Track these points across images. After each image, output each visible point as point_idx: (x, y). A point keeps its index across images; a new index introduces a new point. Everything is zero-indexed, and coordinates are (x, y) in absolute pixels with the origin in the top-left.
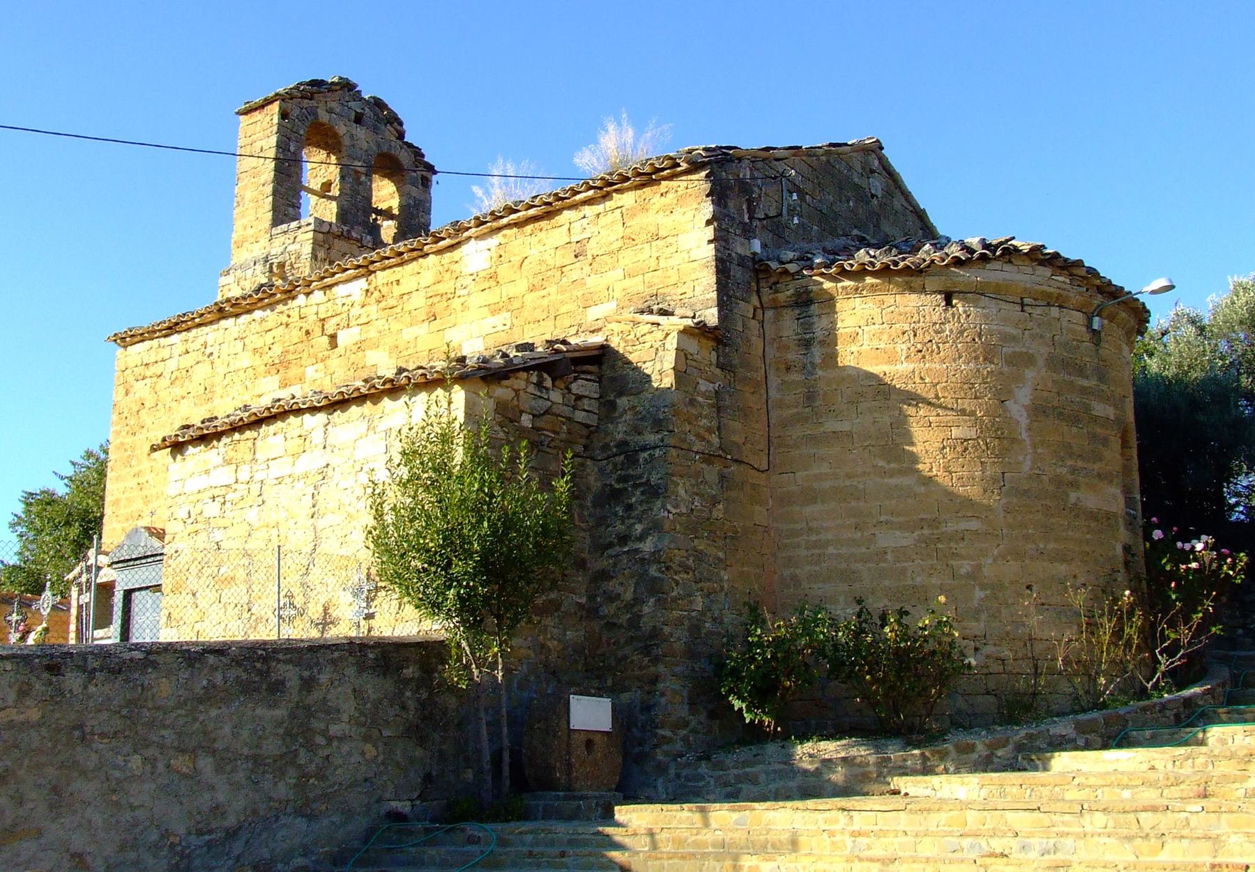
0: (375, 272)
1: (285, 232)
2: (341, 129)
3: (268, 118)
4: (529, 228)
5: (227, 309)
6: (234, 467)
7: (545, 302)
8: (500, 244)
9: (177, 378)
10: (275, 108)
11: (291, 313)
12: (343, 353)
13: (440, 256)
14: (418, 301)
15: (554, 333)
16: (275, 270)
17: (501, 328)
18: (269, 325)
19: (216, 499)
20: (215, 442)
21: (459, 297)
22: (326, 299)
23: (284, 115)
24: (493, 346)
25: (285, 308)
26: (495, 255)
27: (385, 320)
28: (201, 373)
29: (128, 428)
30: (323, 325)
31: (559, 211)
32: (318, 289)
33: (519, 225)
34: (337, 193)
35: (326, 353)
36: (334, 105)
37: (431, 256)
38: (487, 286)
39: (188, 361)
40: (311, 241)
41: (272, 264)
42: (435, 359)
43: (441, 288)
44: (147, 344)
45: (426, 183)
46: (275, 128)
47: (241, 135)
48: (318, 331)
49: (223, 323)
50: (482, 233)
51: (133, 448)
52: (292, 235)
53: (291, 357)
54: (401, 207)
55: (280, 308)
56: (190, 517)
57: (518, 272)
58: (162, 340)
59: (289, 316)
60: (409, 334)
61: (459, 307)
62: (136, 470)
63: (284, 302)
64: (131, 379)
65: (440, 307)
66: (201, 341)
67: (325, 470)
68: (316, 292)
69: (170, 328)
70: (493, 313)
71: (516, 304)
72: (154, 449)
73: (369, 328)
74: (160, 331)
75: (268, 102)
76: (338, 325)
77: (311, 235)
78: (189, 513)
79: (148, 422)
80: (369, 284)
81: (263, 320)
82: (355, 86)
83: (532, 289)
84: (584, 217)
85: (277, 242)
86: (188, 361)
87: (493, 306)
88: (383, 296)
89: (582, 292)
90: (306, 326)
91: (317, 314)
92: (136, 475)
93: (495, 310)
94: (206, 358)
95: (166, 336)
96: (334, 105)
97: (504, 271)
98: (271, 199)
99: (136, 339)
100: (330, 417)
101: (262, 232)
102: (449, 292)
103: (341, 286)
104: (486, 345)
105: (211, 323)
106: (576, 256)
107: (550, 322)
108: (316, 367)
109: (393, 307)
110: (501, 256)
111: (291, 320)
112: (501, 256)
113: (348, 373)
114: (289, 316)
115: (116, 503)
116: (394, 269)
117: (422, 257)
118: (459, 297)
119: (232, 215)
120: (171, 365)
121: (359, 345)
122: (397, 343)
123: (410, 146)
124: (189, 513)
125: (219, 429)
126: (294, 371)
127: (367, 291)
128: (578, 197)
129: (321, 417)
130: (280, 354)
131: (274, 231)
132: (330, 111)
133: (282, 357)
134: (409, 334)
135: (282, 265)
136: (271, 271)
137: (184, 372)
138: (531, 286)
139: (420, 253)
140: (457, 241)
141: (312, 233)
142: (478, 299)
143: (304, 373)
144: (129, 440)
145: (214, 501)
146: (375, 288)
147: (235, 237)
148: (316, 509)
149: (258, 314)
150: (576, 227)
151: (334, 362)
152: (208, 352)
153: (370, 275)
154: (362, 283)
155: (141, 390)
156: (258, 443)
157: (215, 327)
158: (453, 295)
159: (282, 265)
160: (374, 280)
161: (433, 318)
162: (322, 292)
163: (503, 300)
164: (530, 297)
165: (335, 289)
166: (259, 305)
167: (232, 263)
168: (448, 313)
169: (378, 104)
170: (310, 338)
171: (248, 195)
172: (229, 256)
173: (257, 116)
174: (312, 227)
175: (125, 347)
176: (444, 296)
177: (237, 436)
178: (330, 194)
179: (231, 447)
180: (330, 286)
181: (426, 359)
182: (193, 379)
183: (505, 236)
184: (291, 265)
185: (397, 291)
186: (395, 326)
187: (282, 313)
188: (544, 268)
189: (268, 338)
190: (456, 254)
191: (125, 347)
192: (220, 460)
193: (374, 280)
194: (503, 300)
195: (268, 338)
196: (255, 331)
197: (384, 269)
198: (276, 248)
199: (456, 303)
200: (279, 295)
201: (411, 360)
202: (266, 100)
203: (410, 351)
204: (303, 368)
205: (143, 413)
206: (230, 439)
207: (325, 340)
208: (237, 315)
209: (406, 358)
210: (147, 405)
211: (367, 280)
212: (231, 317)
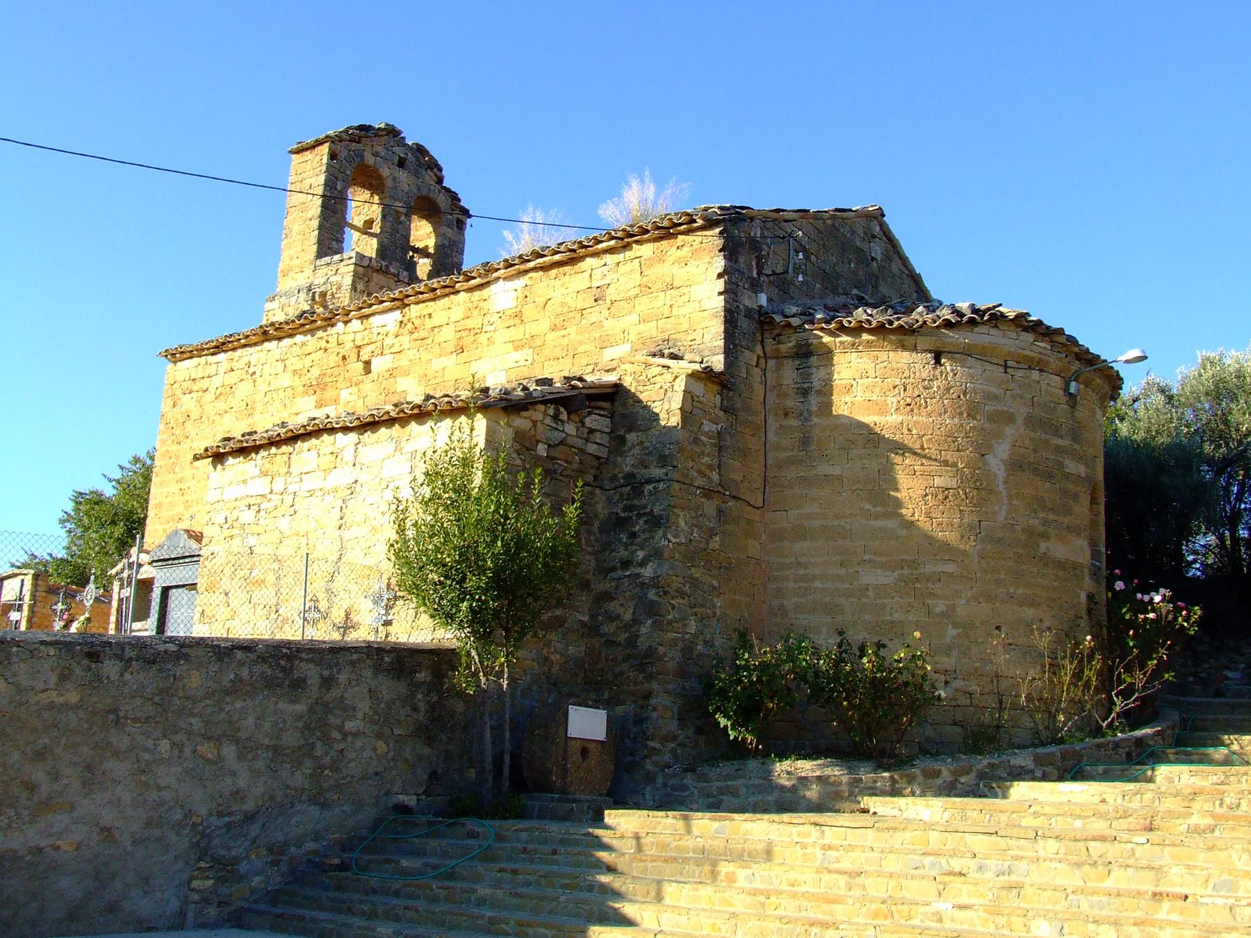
0: (409, 305)
1: (328, 264)
2: (385, 172)
3: (318, 158)
4: (553, 272)
7: (565, 341)
9: (221, 394)
10: (325, 148)
11: (330, 339)
12: (375, 378)
14: (448, 334)
16: (317, 298)
17: (522, 363)
18: (309, 348)
22: (362, 328)
23: (333, 156)
25: (325, 334)
26: (521, 296)
28: (244, 390)
29: (174, 437)
31: (582, 258)
33: (545, 268)
34: (378, 231)
35: (360, 378)
36: (380, 149)
39: (232, 378)
41: (315, 293)
43: (470, 323)
44: (196, 360)
45: (461, 226)
46: (324, 168)
47: (292, 172)
48: (353, 357)
49: (267, 345)
51: (178, 457)
52: (334, 268)
53: (327, 379)
54: (437, 246)
55: (320, 333)
57: (542, 312)
58: (210, 358)
59: (328, 342)
60: (438, 364)
62: (179, 476)
63: (324, 328)
64: (179, 392)
65: (467, 341)
66: (245, 360)
68: (354, 321)
69: (217, 347)
70: (516, 349)
71: (538, 342)
72: (197, 458)
74: (208, 349)
75: (319, 143)
79: (193, 434)
81: (303, 344)
82: (399, 133)
83: (554, 328)
85: (320, 273)
86: (232, 378)
90: (343, 352)
91: (354, 341)
92: (180, 481)
94: (249, 376)
95: (213, 354)
96: (380, 149)
97: (528, 311)
98: (316, 232)
99: (185, 356)
101: (307, 263)
103: (377, 317)
105: (256, 344)
106: (596, 301)
107: (569, 360)
108: (350, 390)
111: (329, 345)
114: (328, 342)
115: (160, 505)
117: (453, 293)
119: (280, 245)
120: (217, 381)
122: (427, 372)
123: (448, 190)
125: (258, 443)
126: (329, 393)
127: (401, 322)
128: (600, 246)
129: (353, 436)
131: (318, 262)
132: (376, 155)
134: (438, 364)
135: (323, 295)
136: (313, 299)
137: (228, 389)
140: (486, 280)
142: (503, 336)
143: (339, 395)
144: (174, 448)
146: (409, 320)
147: (281, 266)
148: (343, 521)
149: (299, 338)
150: (597, 274)
151: (368, 387)
152: (251, 371)
154: (397, 315)
155: (187, 403)
156: (293, 457)
157: (259, 348)
159: (323, 295)
164: (551, 336)
165: (372, 319)
166: (301, 330)
167: (278, 290)
168: (475, 346)
169: (420, 150)
171: (296, 228)
172: (275, 283)
173: (308, 155)
174: (353, 261)
175: (175, 362)
177: (274, 450)
178: (372, 231)
180: (367, 316)
182: (237, 395)
183: (531, 278)
184: (332, 294)
185: (429, 323)
186: (425, 356)
187: (321, 338)
188: (565, 310)
189: (308, 361)
190: (485, 293)
191: (175, 362)
192: (257, 471)
195: (308, 361)
197: (417, 303)
198: (319, 279)
199: (483, 338)
202: (317, 141)
205: (188, 424)
206: (267, 453)
207: (360, 365)
208: (280, 339)
210: (193, 417)
212: (275, 339)
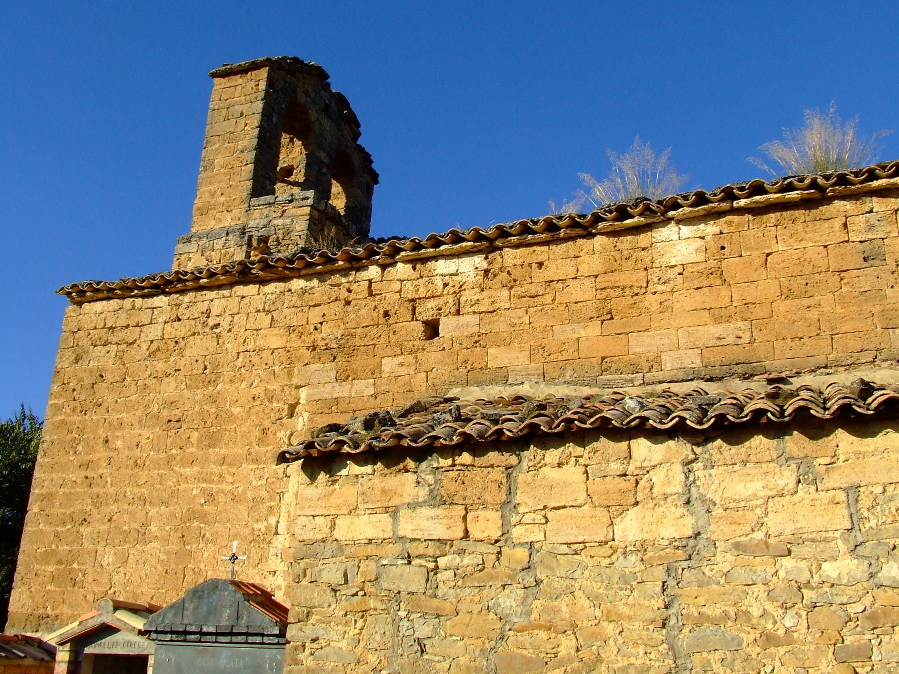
0: (501, 249)
1: (270, 204)
2: (313, 115)
3: (253, 84)
4: (773, 217)
5: (254, 271)
6: (460, 511)
7: (813, 314)
8: (721, 233)
9: (158, 350)
10: (264, 73)
11: (354, 287)
12: (447, 346)
13: (616, 239)
14: (582, 291)
15: (831, 357)
16: (255, 243)
17: (730, 340)
18: (317, 297)
19: (415, 562)
20: (410, 463)
21: (655, 293)
22: (415, 274)
23: (270, 83)
24: (718, 364)
25: (343, 280)
26: (713, 248)
27: (524, 309)
28: (198, 347)
29: (77, 404)
30: (414, 308)
31: (829, 200)
32: (402, 262)
33: (757, 211)
34: (301, 179)
35: (417, 343)
36: (310, 89)
37: (599, 238)
38: (705, 283)
39: (179, 330)
40: (308, 217)
41: (250, 237)
42: (613, 370)
43: (622, 278)
44: (114, 303)
45: (369, 192)
46: (262, 95)
47: (214, 97)
48: (405, 313)
49: (240, 289)
50: (697, 214)
51: (82, 431)
52: (280, 209)
53: (357, 342)
54: (347, 207)
55: (336, 278)
56: (346, 582)
57: (762, 270)
58: (139, 301)
59: (349, 291)
60: (566, 333)
61: (655, 307)
62: (86, 458)
63: (345, 272)
64: (85, 342)
65: (620, 303)
66: (203, 306)
67: (692, 542)
68: (399, 265)
69: (156, 286)
70: (717, 320)
71: (759, 312)
72: (283, 458)
73: (495, 318)
74: (143, 288)
75: (255, 66)
76: (440, 309)
77: (307, 210)
78: (345, 575)
79: (109, 399)
80: (490, 263)
81: (304, 291)
82: (327, 77)
83: (787, 294)
84: (871, 211)
85: (256, 214)
86: (179, 330)
87: (717, 311)
88: (515, 280)
89: (881, 308)
90: (384, 306)
91: (400, 291)
92: (88, 465)
93: (719, 316)
94: (207, 329)
95: (144, 296)
96: (310, 89)
97: (731, 265)
98: (251, 167)
99: (100, 295)
100: (698, 450)
101: (237, 202)
102: (636, 284)
103: (441, 262)
104: (705, 360)
105: (220, 287)
106: (865, 259)
107: (825, 343)
108: (400, 359)
109: (537, 296)
110: (723, 248)
111: (352, 296)
112: (723, 248)
113: (456, 373)
114: (349, 291)
115: (49, 498)
116: (535, 248)
117: (583, 237)
118: (655, 293)
119: (196, 179)
120: (153, 332)
121: (477, 339)
122: (544, 342)
123: (361, 150)
124: (345, 575)
125: (405, 443)
126: (359, 362)
127: (487, 271)
128: (875, 184)
129: (679, 448)
130: (338, 335)
131: (254, 201)
132: (307, 94)
133: (343, 341)
134: (566, 333)
135: (264, 240)
136: (249, 245)
137: (171, 344)
138: (785, 290)
139: (585, 232)
140: (649, 221)
141: (309, 208)
142: (685, 300)
143: (380, 366)
144: (76, 418)
145: (409, 563)
146: (501, 269)
147: (198, 203)
148: (672, 611)
149: (297, 284)
150: (857, 223)
151: (432, 354)
152: (211, 322)
153: (492, 252)
154: (479, 260)
155: (100, 358)
156: (522, 478)
157: (226, 292)
158: (643, 290)
159: (264, 240)
160: (499, 259)
161: (609, 316)
162: (409, 266)
163: (735, 304)
164: (782, 306)
165: (431, 264)
166: (303, 272)
167: (194, 230)
168: (635, 312)
169: (342, 101)
170: (390, 322)
171: (219, 161)
172: (188, 222)
173: (238, 80)
174: (310, 202)
175: (80, 304)
176: (628, 290)
177: (466, 458)
178: (289, 179)
179: (452, 474)
180: (424, 260)
181: (597, 368)
182: (187, 353)
183: (729, 223)
184: (277, 240)
185: (540, 276)
186: (541, 322)
187: (339, 285)
188: (807, 269)
189: (315, 315)
190: (643, 239)
191: (80, 304)
192: (422, 493)
193: (499, 259)
194: (735, 304)
195: (315, 315)
196: (292, 303)
197: (517, 246)
198: (256, 220)
199: (650, 300)
200: (340, 263)
201: (569, 368)
202: (253, 63)
203: (566, 356)
204: (377, 359)
205: (102, 387)
206: (449, 461)
207: (418, 328)
208: (263, 282)
209: (561, 364)
210: (109, 377)
211: (487, 258)
212: (254, 282)
